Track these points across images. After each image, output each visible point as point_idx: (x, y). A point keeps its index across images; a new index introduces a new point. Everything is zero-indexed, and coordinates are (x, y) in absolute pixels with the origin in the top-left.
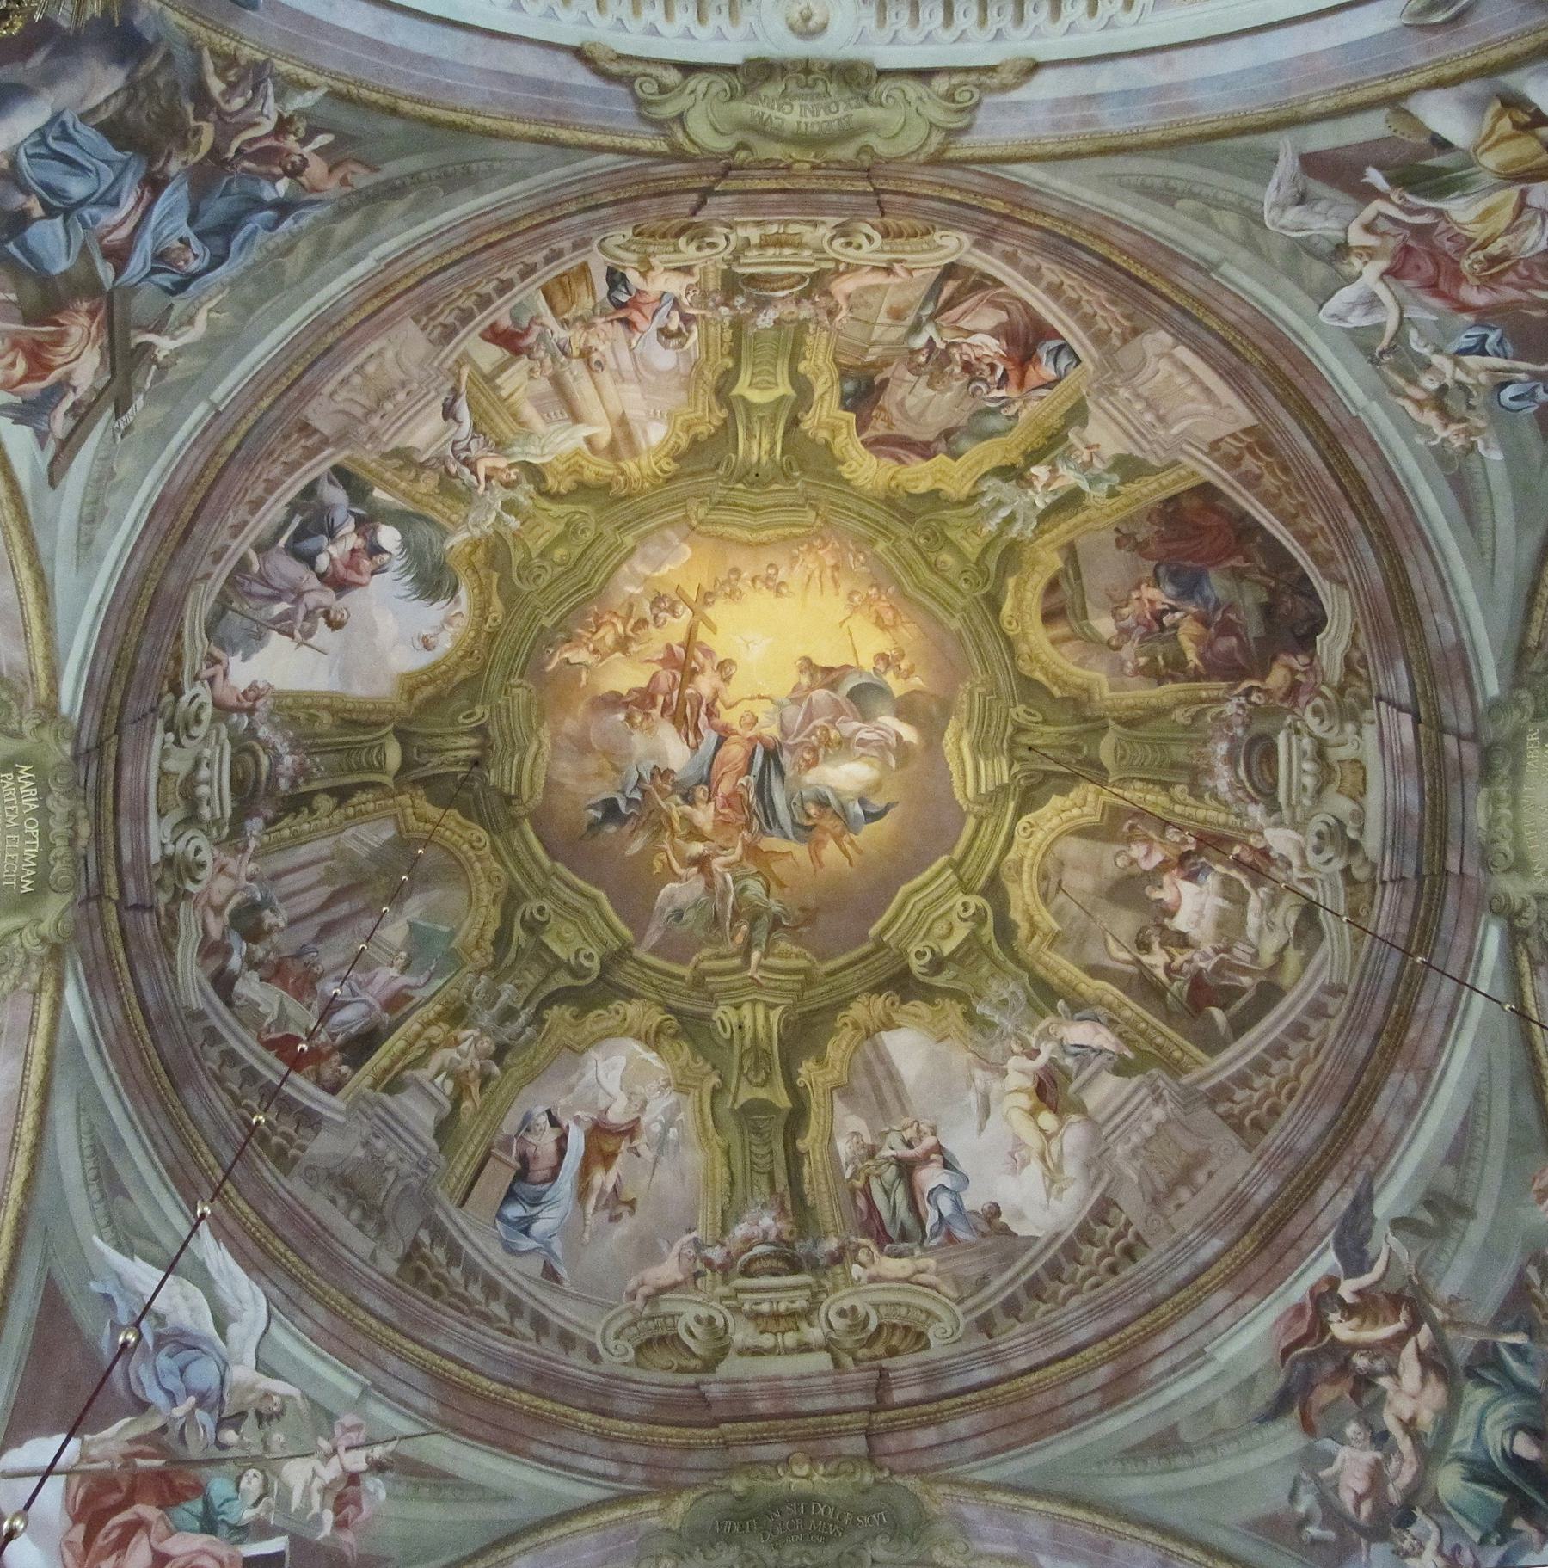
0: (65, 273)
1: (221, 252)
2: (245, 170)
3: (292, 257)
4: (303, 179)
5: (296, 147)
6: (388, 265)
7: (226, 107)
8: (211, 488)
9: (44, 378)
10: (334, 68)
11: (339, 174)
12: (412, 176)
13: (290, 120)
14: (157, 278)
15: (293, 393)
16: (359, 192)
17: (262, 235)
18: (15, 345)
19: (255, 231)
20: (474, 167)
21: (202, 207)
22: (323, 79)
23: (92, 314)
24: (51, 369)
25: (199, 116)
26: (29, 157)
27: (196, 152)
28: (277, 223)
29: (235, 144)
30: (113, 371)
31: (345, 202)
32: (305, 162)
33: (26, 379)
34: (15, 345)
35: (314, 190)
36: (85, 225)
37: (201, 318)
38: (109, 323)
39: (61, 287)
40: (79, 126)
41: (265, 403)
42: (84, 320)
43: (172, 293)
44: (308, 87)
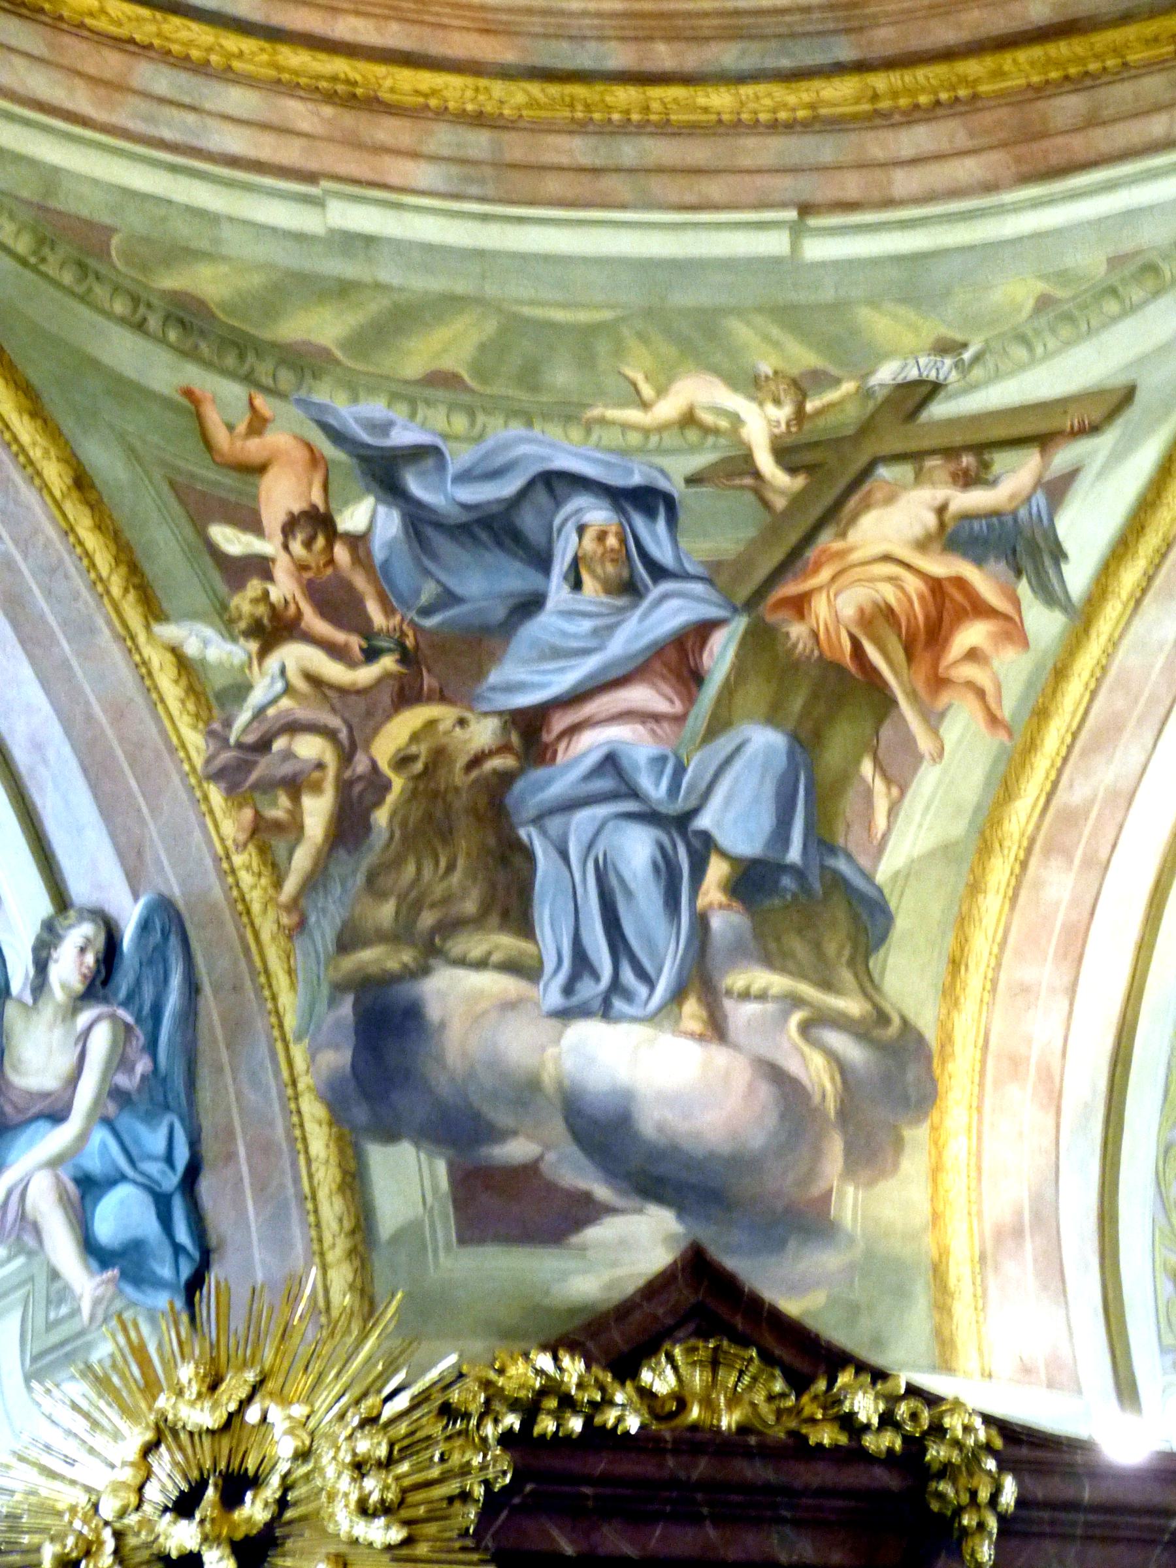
0: (772, 719)
1: (541, 496)
2: (388, 611)
3: (448, 363)
4: (317, 497)
5: (282, 570)
6: (311, 177)
7: (330, 758)
8: (948, 55)
9: (960, 583)
10: (116, 652)
11: (254, 449)
12: (140, 327)
13: (256, 630)
14: (663, 553)
15: (664, 56)
16: (249, 379)
17: (460, 457)
18: (939, 683)
19: (465, 477)
20: (23, 246)
21: (499, 613)
22: (148, 651)
23: (799, 605)
24: (936, 586)
25: (378, 785)
26: (651, 983)
27: (431, 724)
28: (417, 453)
29: (366, 674)
30: (866, 472)
31: (286, 378)
32: (290, 527)
33: (980, 609)
34: (939, 683)
35: (315, 459)
36: (680, 770)
37: (667, 409)
39: (797, 704)
40: (549, 965)
41: (720, 99)
42: (820, 607)
43: (670, 503)
44: (183, 664)
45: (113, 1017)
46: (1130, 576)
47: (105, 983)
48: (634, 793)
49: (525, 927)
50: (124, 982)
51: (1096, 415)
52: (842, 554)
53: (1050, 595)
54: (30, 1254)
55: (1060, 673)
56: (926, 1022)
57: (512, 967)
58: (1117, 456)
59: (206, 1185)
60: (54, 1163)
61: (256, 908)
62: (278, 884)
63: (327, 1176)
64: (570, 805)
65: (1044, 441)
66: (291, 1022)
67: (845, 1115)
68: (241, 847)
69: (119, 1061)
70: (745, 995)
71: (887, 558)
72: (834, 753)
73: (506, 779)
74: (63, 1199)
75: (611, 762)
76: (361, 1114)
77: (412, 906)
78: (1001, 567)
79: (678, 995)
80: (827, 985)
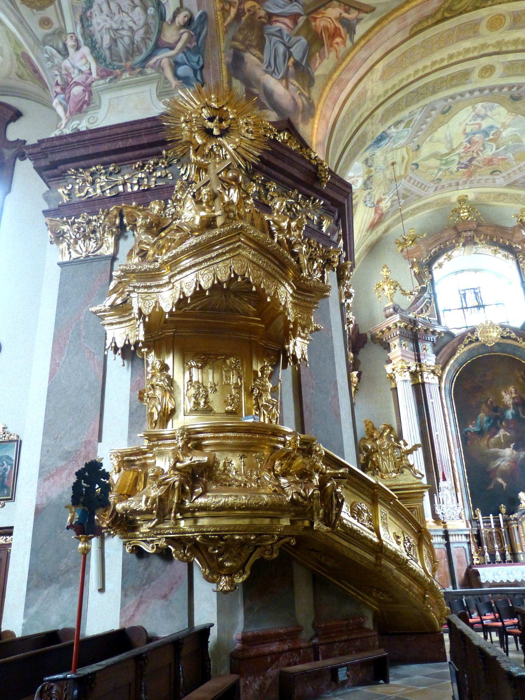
0: (306, 38)
9: (339, 29)
18: (331, 46)
23: (315, 19)
24: (336, 28)
27: (255, 6)
33: (341, 36)
36: (290, 39)
38: (315, 11)
39: (310, 37)
42: (318, 20)
45: (189, 32)
46: (362, 43)
47: (189, 25)
48: (282, 38)
49: (262, 52)
50: (193, 26)
51: (368, 10)
52: (324, 13)
53: (351, 39)
54: (160, 73)
55: (348, 54)
56: (316, 102)
57: (259, 58)
58: (370, 19)
59: (204, 71)
60: (169, 57)
61: (220, 24)
62: (224, 21)
63: (225, 80)
64: (273, 35)
65: (359, 10)
66: (222, 49)
67: (303, 111)
68: (220, 11)
69: (189, 41)
70: (292, 84)
71: (330, 18)
72: (314, 49)
73: (264, 24)
74: (170, 65)
75: (280, 31)
76: (232, 71)
77: (245, 38)
78: (346, 30)
79: (282, 78)
80: (304, 89)
